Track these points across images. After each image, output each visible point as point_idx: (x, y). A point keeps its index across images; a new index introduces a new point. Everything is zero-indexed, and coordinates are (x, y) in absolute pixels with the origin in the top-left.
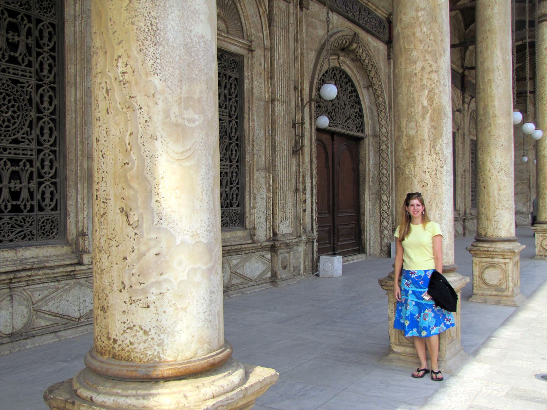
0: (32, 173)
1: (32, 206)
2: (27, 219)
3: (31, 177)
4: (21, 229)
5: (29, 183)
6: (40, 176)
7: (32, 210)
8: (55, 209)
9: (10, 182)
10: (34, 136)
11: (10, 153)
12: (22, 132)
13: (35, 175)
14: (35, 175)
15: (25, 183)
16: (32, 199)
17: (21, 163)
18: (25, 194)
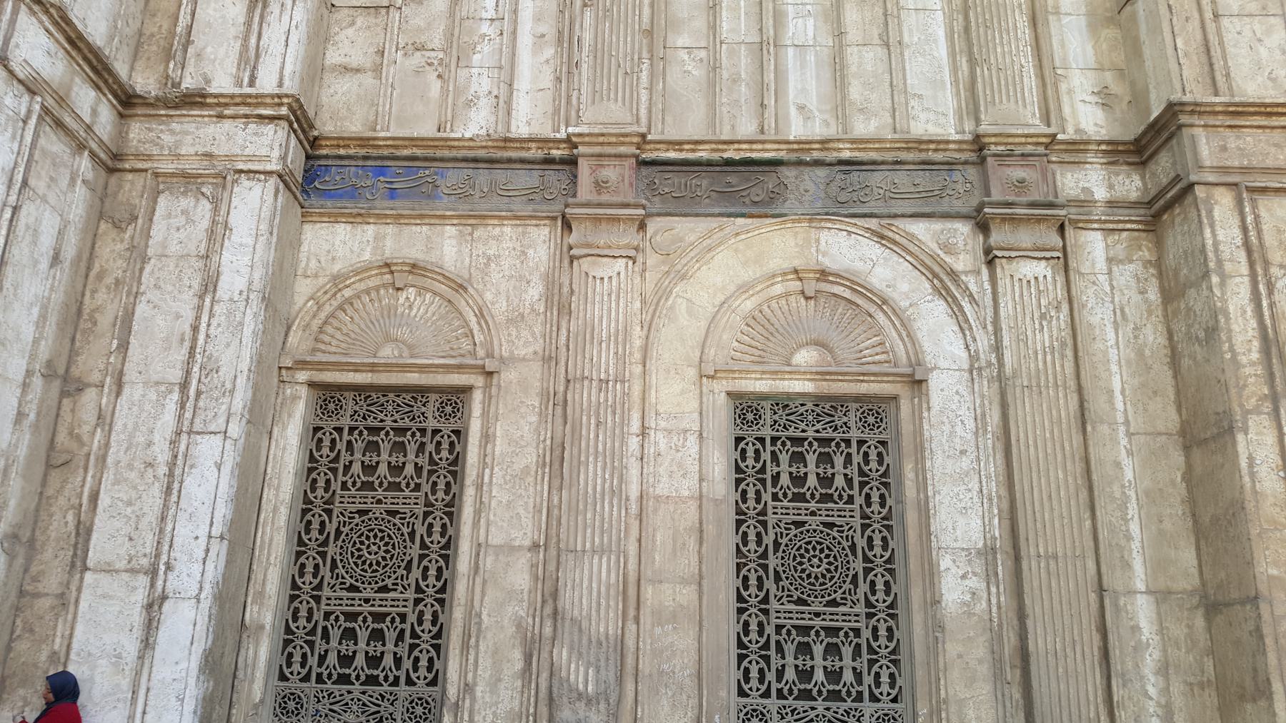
0: (402, 631)
1: (397, 679)
2: (388, 696)
3: (401, 637)
4: (377, 709)
5: (396, 645)
6: (414, 635)
7: (396, 682)
8: (433, 683)
9: (340, 643)
10: (412, 580)
11: (373, 605)
12: (394, 577)
13: (408, 633)
14: (408, 633)
15: (390, 646)
16: (398, 668)
17: (842, 633)
18: (388, 661)
